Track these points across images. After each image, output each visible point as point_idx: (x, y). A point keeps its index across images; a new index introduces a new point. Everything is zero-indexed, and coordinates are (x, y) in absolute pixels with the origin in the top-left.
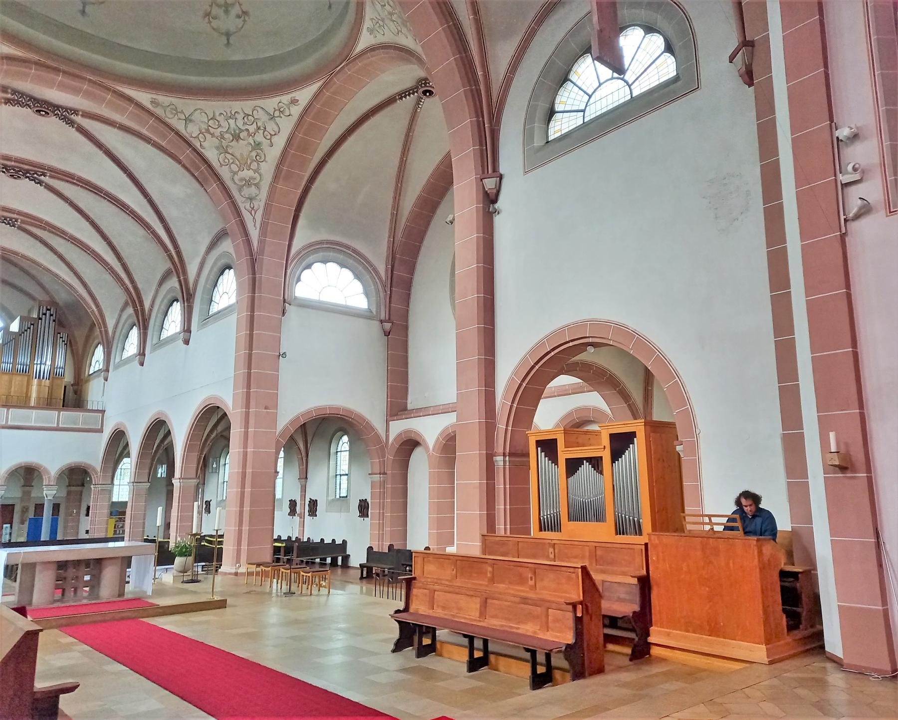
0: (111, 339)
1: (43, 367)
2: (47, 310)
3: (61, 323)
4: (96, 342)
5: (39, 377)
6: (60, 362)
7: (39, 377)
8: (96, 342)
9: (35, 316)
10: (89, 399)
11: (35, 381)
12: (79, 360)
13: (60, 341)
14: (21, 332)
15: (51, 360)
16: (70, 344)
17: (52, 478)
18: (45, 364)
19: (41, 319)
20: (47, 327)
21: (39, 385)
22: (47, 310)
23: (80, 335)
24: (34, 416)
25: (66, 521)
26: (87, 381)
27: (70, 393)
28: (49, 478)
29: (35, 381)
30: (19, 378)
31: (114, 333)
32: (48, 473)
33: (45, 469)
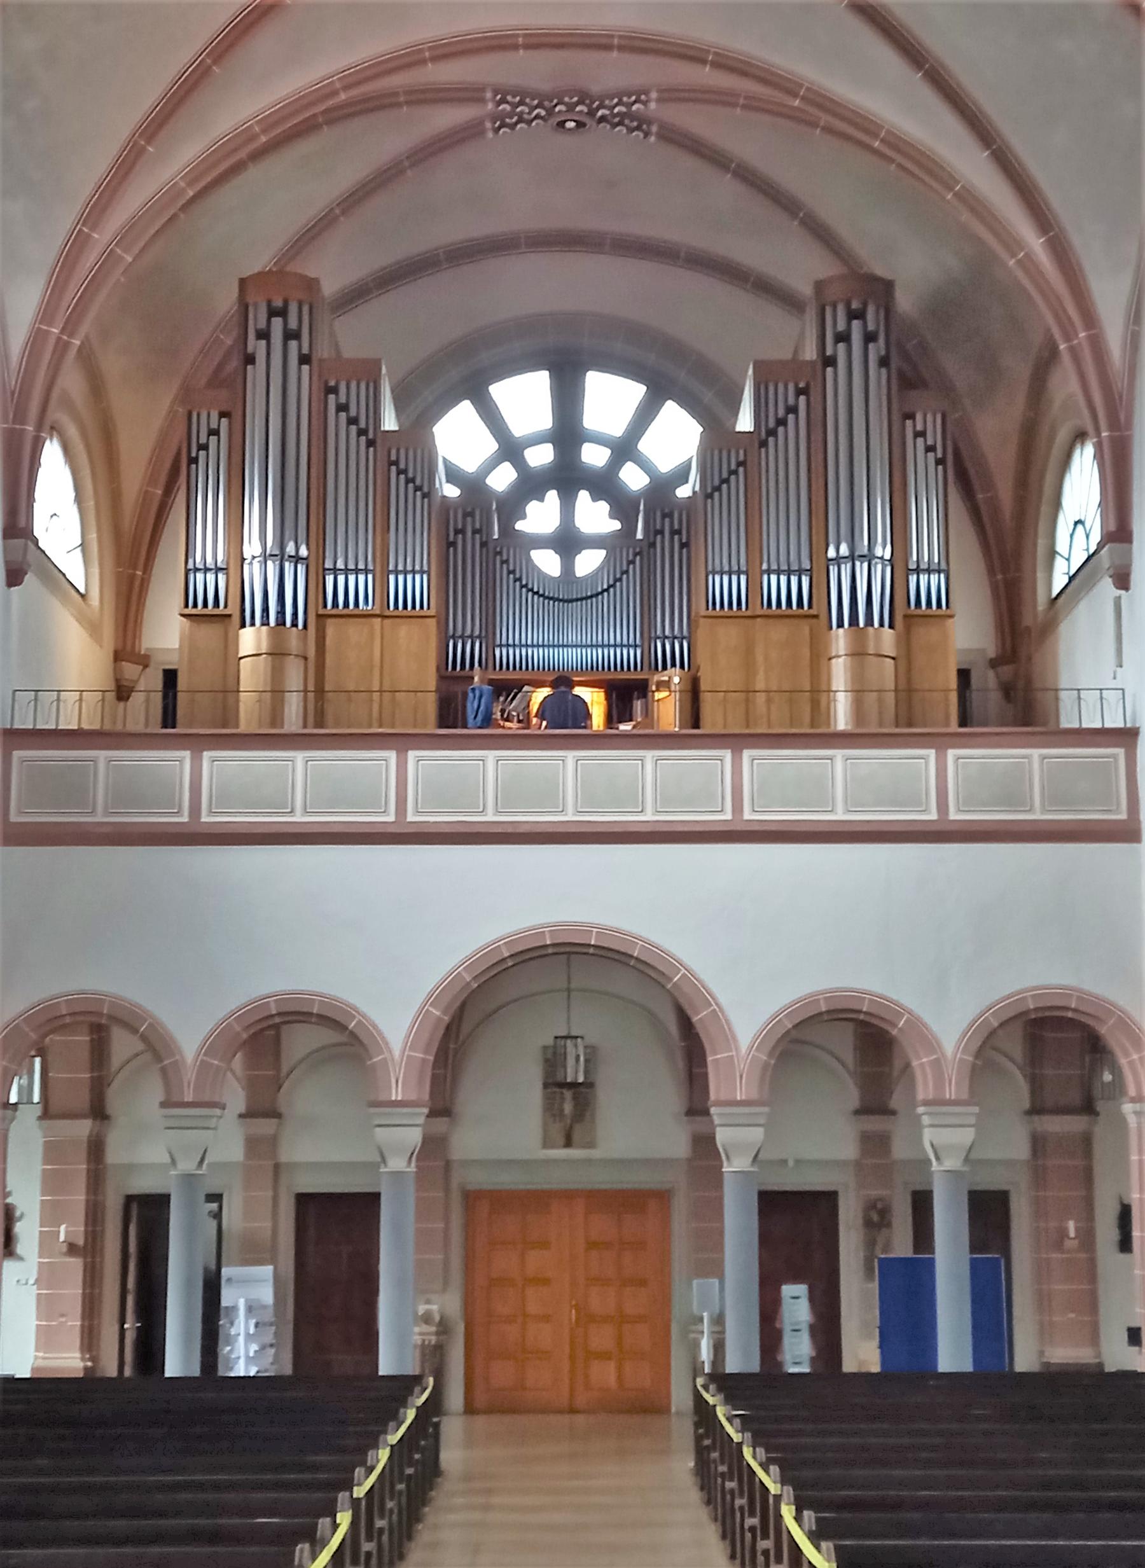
0: (1120, 383)
1: (862, 569)
2: (852, 315)
3: (910, 376)
4: (1063, 435)
5: (854, 620)
6: (926, 544)
7: (854, 620)
8: (1063, 435)
9: (810, 353)
10: (1064, 683)
11: (840, 640)
12: (1007, 537)
13: (915, 450)
14: (764, 435)
15: (899, 545)
16: (963, 473)
17: (952, 1072)
18: (869, 558)
19: (830, 361)
20: (857, 389)
21: (858, 654)
22: (852, 315)
23: (994, 433)
24: (843, 779)
25: (1042, 1271)
26: (1049, 627)
27: (986, 681)
28: (937, 1064)
29: (840, 640)
30: (778, 632)
31: (1133, 343)
32: (931, 1043)
33: (915, 1023)
